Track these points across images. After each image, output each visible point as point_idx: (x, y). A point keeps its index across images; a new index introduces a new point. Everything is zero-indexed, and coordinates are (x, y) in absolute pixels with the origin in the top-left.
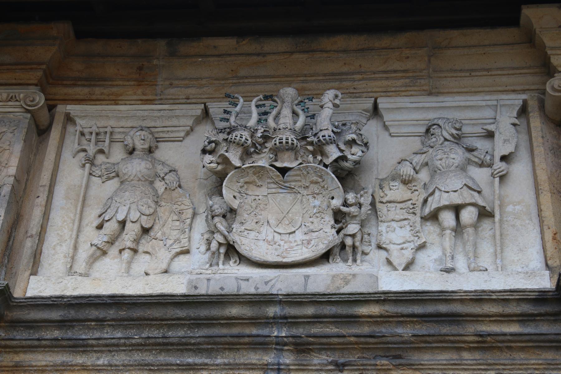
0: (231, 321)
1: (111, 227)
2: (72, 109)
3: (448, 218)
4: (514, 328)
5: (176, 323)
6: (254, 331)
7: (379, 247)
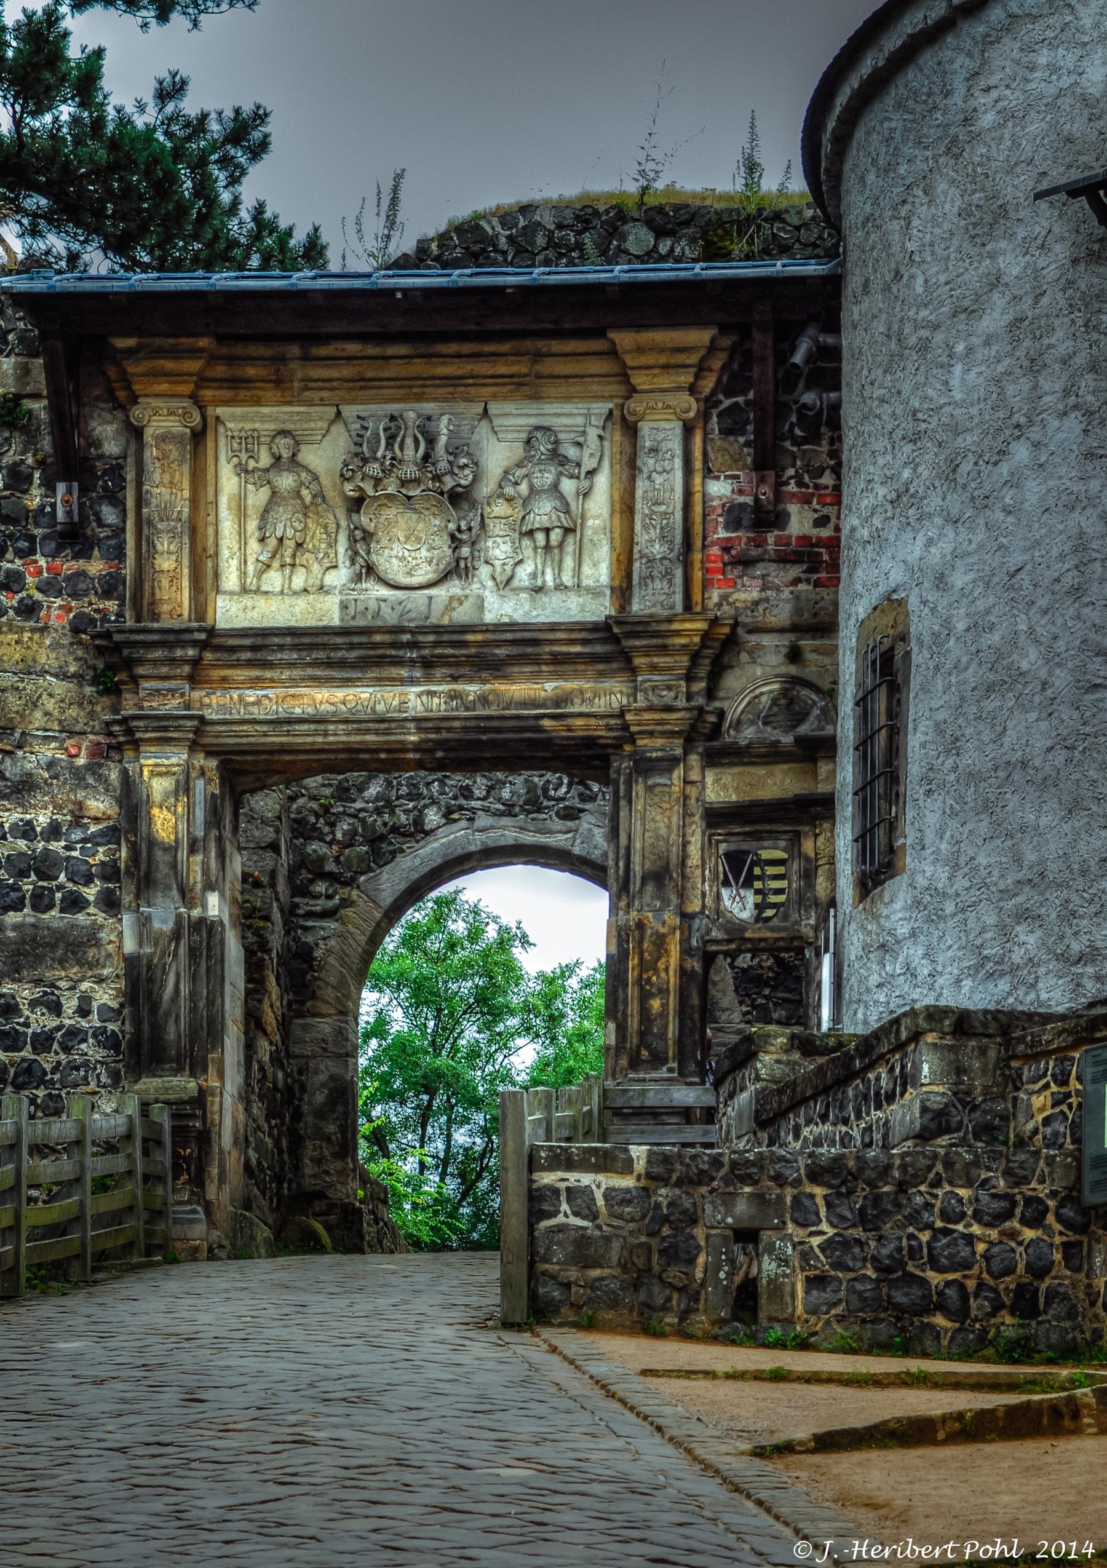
0: (375, 646)
1: (272, 542)
2: (220, 411)
3: (540, 537)
4: (577, 649)
5: (336, 648)
6: (393, 653)
7: (487, 562)
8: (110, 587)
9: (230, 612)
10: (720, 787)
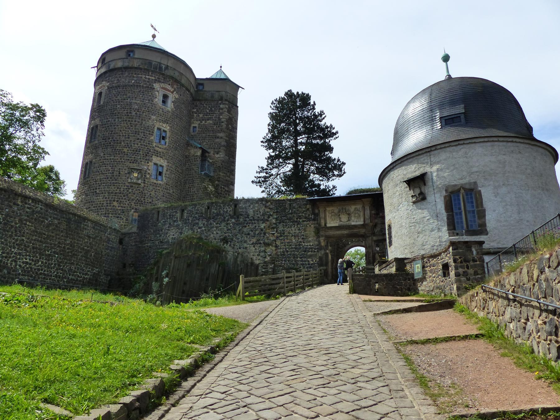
8: (317, 223)
9: (328, 225)
10: (375, 238)
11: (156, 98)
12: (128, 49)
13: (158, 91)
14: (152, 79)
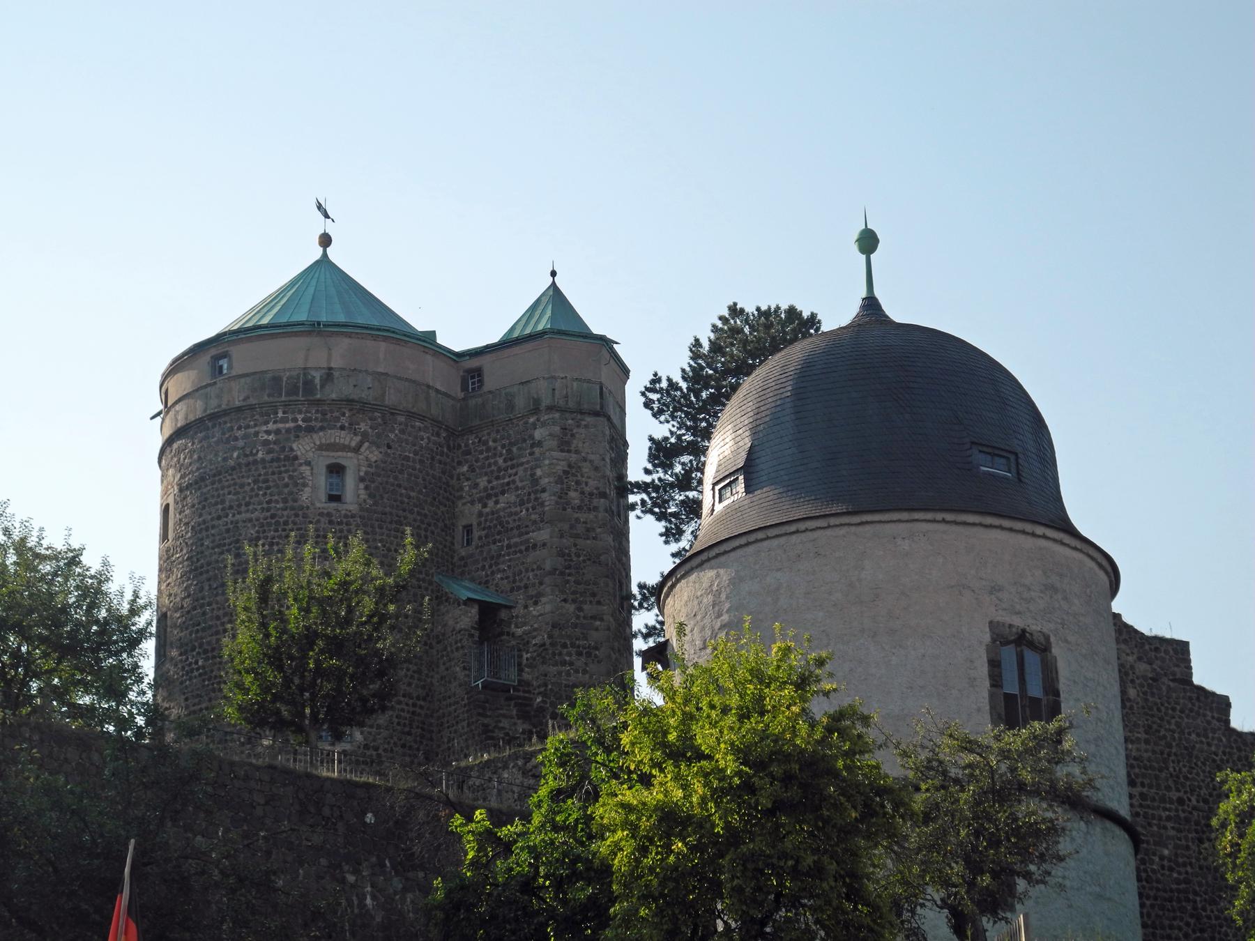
11: (305, 485)
12: (213, 352)
13: (308, 463)
14: (288, 431)
